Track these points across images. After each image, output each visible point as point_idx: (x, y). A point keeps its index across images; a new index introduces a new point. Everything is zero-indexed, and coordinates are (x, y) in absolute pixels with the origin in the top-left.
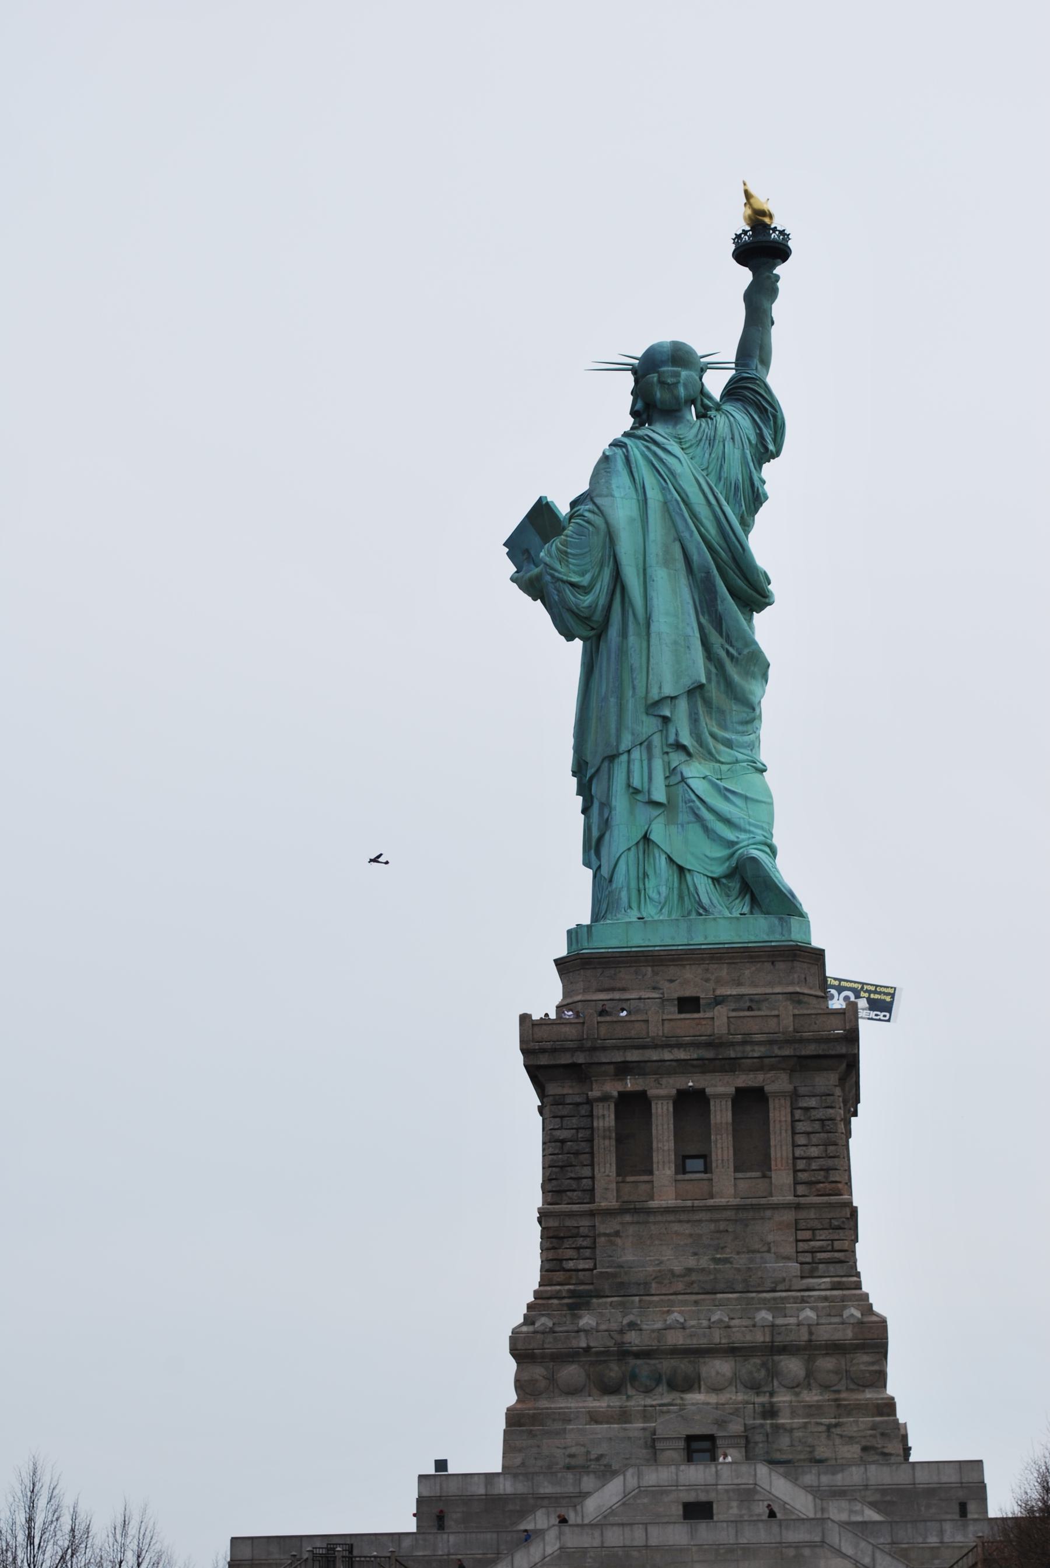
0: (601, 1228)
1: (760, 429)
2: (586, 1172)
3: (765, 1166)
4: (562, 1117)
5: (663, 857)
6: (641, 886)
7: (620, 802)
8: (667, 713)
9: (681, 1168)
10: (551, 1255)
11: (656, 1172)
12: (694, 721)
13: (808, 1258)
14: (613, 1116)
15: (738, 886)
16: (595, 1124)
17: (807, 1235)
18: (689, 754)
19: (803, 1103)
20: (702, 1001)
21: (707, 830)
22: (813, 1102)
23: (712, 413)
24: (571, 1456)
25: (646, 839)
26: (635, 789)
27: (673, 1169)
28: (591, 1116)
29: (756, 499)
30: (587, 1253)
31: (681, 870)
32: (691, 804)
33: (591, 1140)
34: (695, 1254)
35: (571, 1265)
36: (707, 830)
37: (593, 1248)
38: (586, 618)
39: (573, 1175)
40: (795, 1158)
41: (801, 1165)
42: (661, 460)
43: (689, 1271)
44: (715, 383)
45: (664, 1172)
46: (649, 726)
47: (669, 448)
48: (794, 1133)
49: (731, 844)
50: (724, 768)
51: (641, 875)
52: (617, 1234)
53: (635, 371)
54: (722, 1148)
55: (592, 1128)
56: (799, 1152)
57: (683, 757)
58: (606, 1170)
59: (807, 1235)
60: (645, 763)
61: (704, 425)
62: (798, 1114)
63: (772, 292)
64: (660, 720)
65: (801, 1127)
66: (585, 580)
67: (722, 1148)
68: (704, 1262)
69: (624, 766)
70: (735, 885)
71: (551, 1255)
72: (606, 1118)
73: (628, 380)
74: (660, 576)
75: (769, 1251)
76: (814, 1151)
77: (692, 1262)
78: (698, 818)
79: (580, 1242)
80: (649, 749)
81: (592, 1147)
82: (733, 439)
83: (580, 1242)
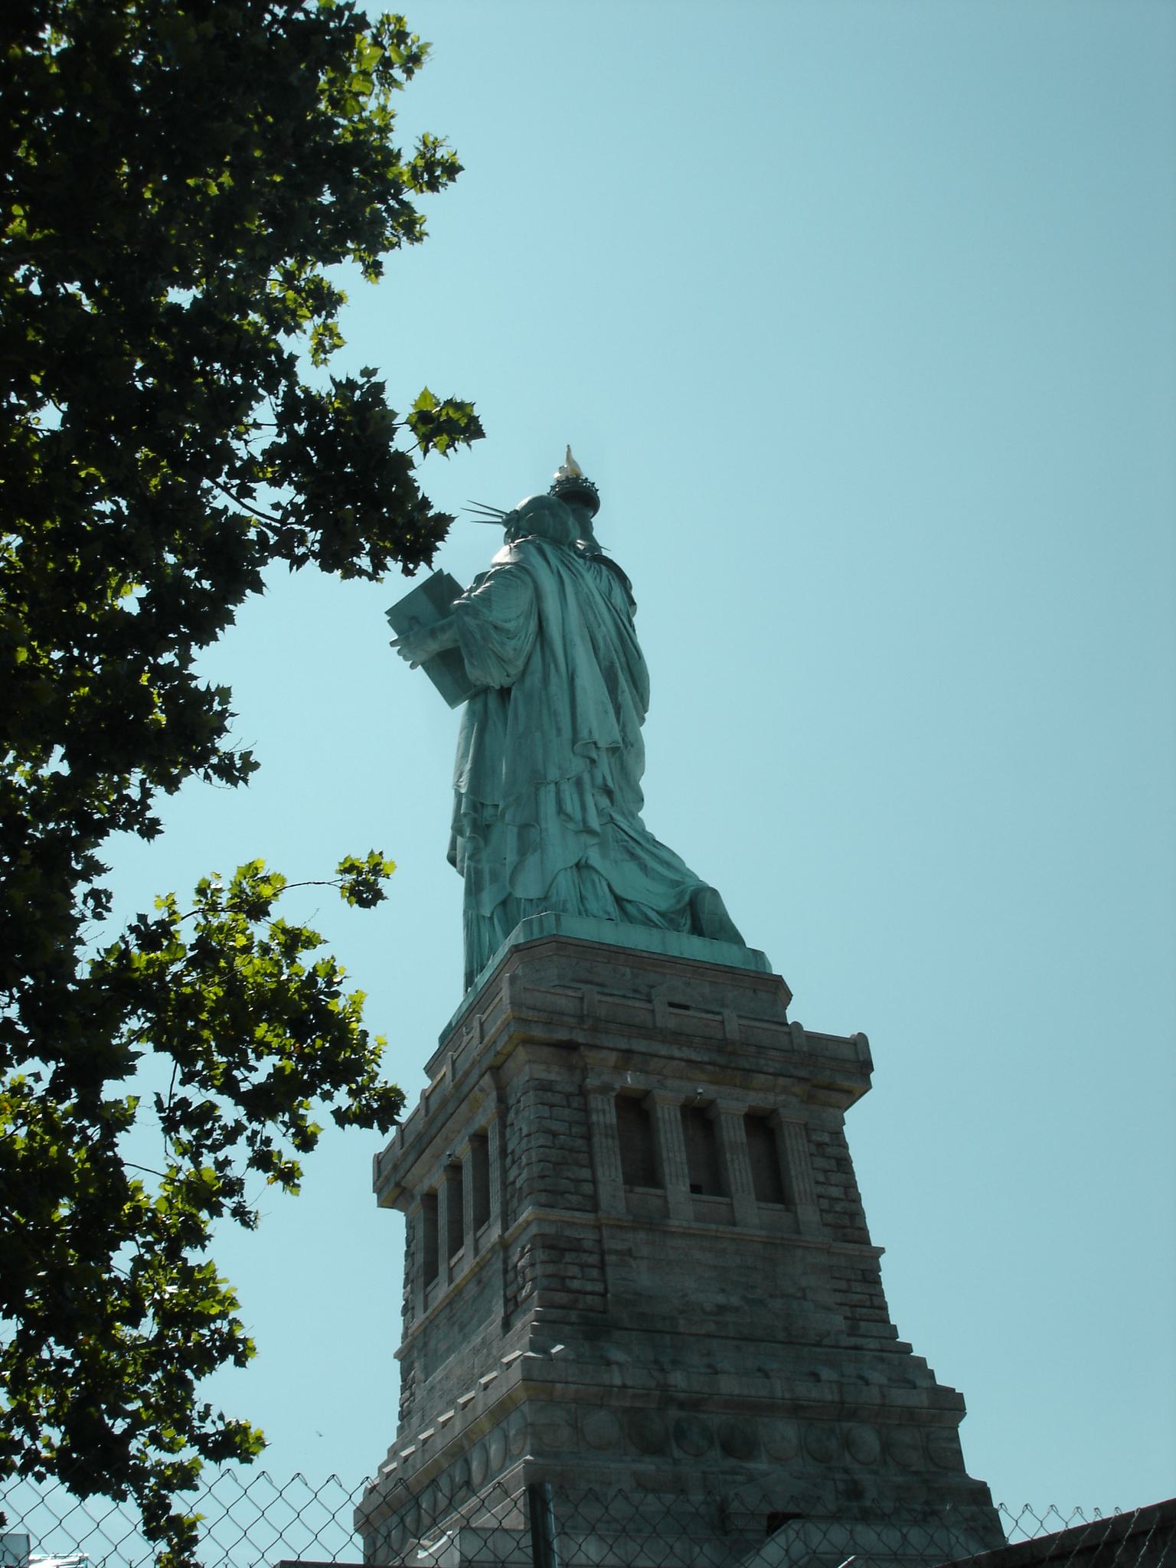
0: (610, 1244)
2: (585, 1173)
4: (552, 1106)
5: (604, 883)
7: (551, 825)
10: (550, 1269)
11: (669, 1186)
13: (848, 1312)
16: (594, 1118)
17: (843, 1285)
22: (826, 1138)
26: (567, 815)
32: (625, 843)
33: (588, 1138)
34: (723, 1291)
35: (576, 1284)
39: (570, 1174)
43: (721, 1309)
45: (678, 1188)
46: (578, 765)
52: (629, 1252)
54: (740, 1171)
58: (610, 1174)
59: (843, 1285)
67: (740, 1171)
68: (735, 1301)
69: (553, 795)
70: (686, 922)
71: (550, 1269)
72: (605, 1114)
74: (578, 640)
75: (804, 1298)
77: (721, 1299)
78: (633, 856)
79: (586, 1258)
83: (586, 1258)
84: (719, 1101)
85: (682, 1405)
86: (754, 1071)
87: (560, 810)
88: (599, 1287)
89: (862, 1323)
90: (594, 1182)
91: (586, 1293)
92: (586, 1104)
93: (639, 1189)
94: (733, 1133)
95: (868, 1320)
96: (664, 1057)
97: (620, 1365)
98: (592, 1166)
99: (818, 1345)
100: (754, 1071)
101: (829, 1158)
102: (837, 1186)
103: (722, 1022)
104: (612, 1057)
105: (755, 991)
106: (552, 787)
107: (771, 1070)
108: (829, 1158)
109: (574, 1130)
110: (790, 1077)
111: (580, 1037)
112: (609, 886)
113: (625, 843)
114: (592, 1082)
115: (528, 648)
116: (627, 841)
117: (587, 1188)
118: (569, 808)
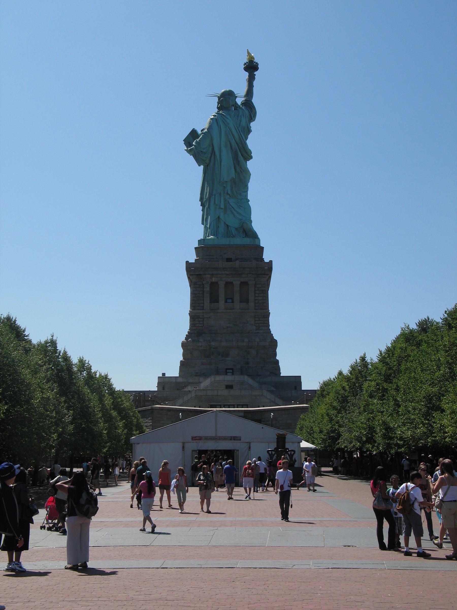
1: (250, 113)
2: (202, 302)
3: (247, 301)
5: (223, 222)
6: (217, 230)
8: (225, 185)
9: (226, 302)
11: (220, 302)
12: (232, 188)
14: (209, 288)
15: (242, 230)
16: (204, 290)
18: (230, 196)
19: (257, 286)
20: (232, 259)
21: (234, 215)
23: (238, 109)
24: (197, 373)
25: (219, 217)
27: (224, 302)
28: (203, 288)
29: (249, 131)
30: (202, 322)
31: (227, 225)
34: (229, 323)
35: (197, 325)
36: (234, 215)
37: (203, 321)
38: (204, 160)
40: (255, 300)
41: (257, 301)
42: (225, 120)
44: (239, 101)
47: (227, 117)
48: (255, 293)
49: (241, 220)
50: (239, 200)
51: (217, 227)
52: (209, 318)
53: (219, 97)
54: (237, 297)
55: (203, 291)
56: (256, 298)
57: (228, 196)
60: (219, 198)
61: (236, 111)
62: (256, 289)
63: (254, 78)
64: (223, 187)
65: (257, 292)
66: (204, 151)
67: (237, 297)
73: (216, 99)
74: (224, 149)
76: (260, 298)
80: (220, 194)
81: (204, 296)
82: (243, 115)
83: (200, 319)
84: (233, 282)
85: (214, 348)
86: (242, 274)
87: (215, 203)
88: (202, 325)
89: (261, 327)
90: (203, 303)
91: (199, 327)
92: (204, 286)
93: (213, 304)
94: (237, 289)
95: (262, 326)
96: (221, 274)
97: (201, 342)
98: (203, 300)
99: (249, 333)
100: (242, 274)
101: (260, 290)
102: (261, 297)
103: (235, 264)
104: (209, 276)
105: (251, 250)
106: (214, 196)
107: (246, 273)
108: (260, 290)
109: (200, 292)
110: (251, 274)
111: (201, 273)
112: (225, 223)
113: (230, 209)
114: (204, 282)
115: (209, 156)
116: (231, 208)
117: (202, 305)
118: (217, 203)
